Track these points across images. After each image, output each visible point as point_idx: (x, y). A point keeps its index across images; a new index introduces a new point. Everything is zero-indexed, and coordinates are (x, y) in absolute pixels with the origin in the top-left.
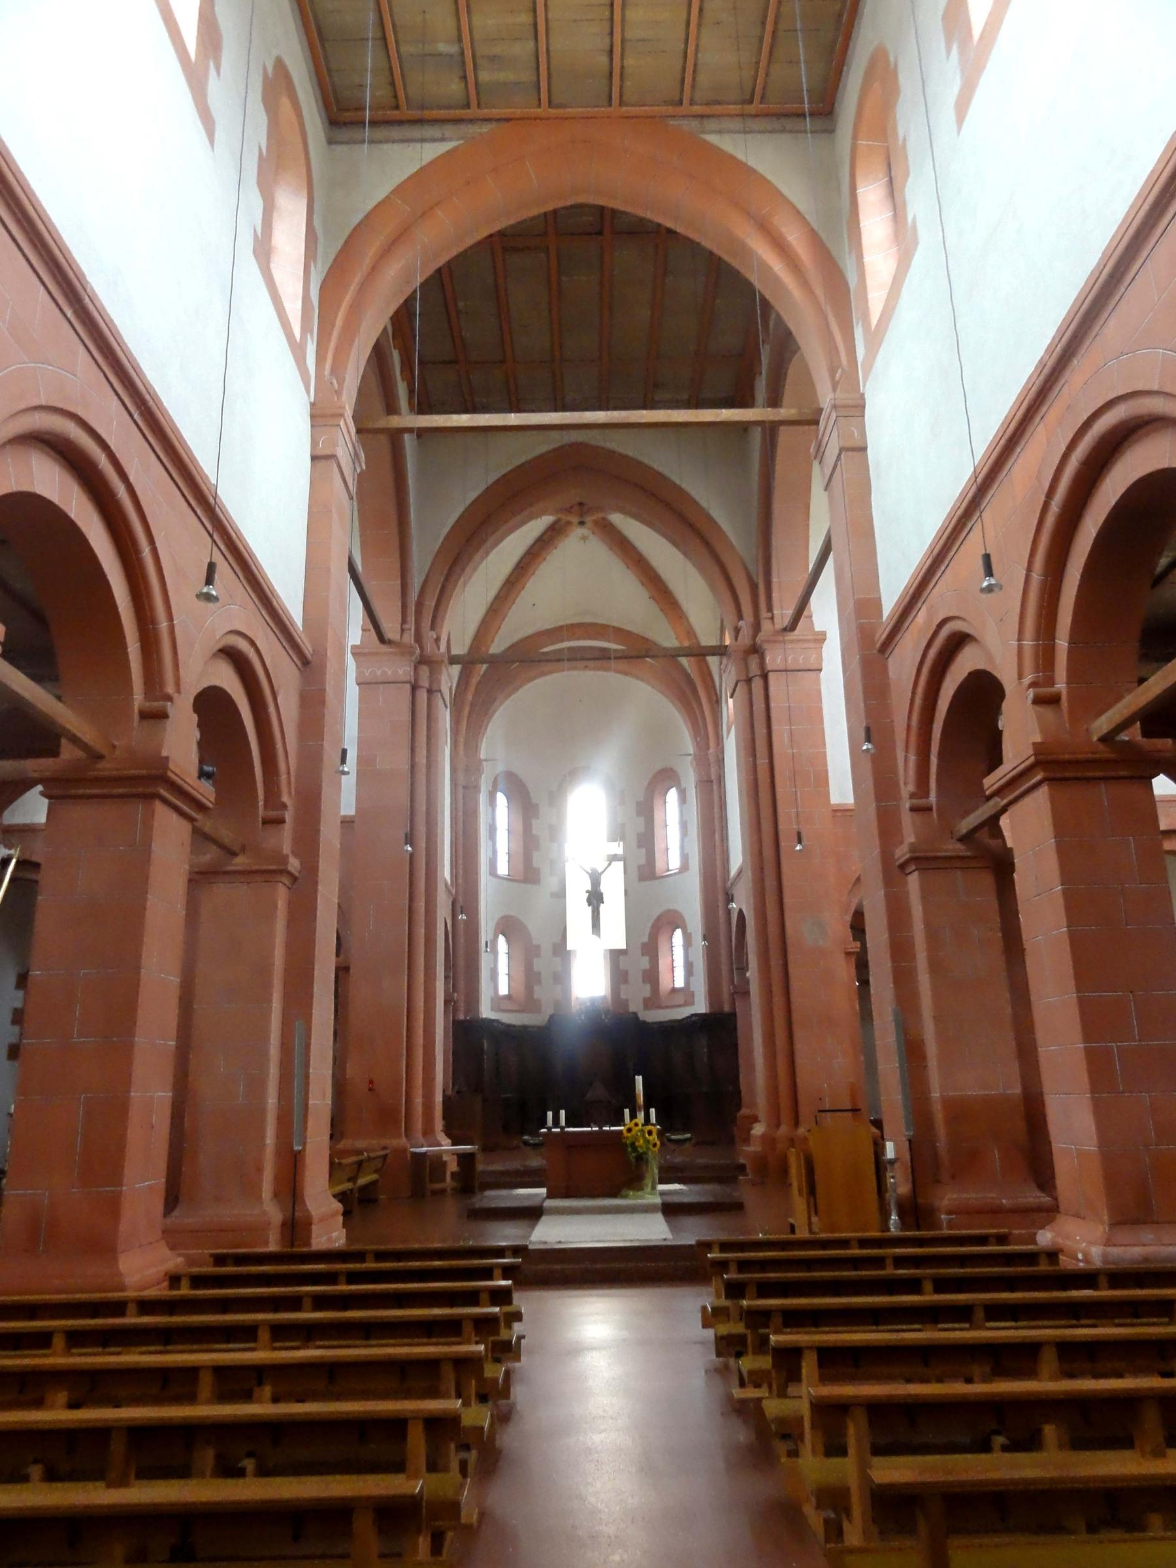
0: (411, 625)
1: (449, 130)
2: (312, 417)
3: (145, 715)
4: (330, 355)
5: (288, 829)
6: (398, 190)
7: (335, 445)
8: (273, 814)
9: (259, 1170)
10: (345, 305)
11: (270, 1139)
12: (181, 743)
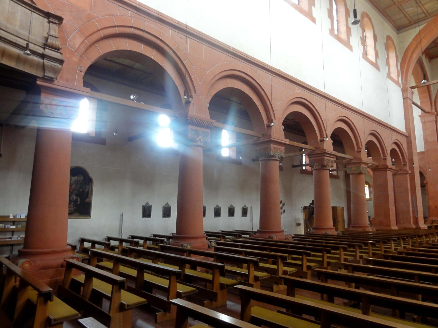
0: (434, 108)
1: (424, 22)
2: (402, 91)
3: (383, 159)
4: (404, 78)
5: (408, 166)
6: (414, 39)
7: (407, 95)
8: (405, 164)
9: (410, 219)
10: (405, 67)
11: (411, 215)
12: (389, 162)
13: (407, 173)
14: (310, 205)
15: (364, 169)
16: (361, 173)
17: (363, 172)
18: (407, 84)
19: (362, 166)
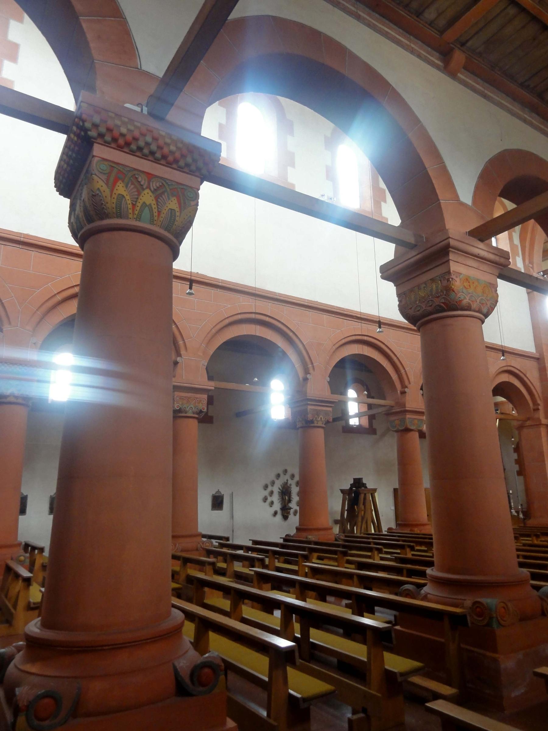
8: (536, 407)
13: (540, 424)
14: (351, 488)
15: (416, 421)
16: (407, 430)
17: (412, 428)
18: (532, 268)
19: (408, 416)
